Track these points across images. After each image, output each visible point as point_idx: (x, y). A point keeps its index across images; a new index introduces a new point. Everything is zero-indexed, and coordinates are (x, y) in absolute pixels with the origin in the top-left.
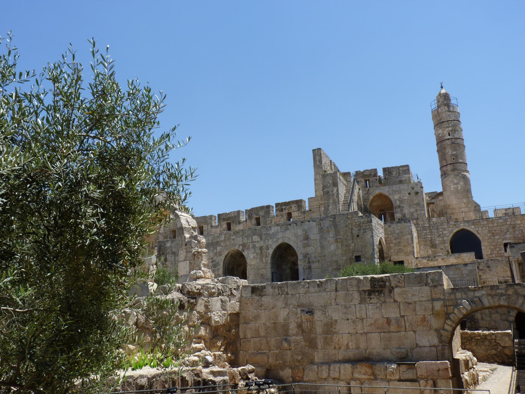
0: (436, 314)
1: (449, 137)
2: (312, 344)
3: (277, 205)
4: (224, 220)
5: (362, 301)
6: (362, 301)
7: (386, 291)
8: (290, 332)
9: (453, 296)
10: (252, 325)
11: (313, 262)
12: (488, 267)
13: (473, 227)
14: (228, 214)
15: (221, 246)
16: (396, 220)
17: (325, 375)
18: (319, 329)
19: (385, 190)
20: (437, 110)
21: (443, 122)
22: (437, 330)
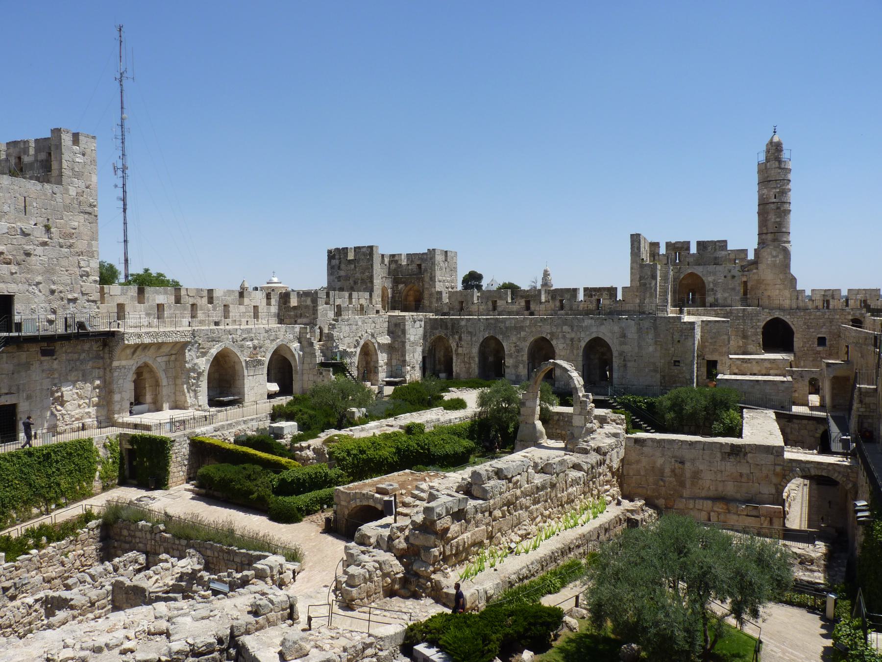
0: (776, 474)
1: (774, 200)
2: (682, 484)
3: (586, 289)
4: (522, 297)
5: (723, 459)
6: (723, 459)
7: (742, 454)
8: (665, 474)
9: (790, 465)
10: (634, 466)
11: (629, 361)
12: (802, 377)
13: (788, 317)
14: (528, 291)
15: (525, 331)
16: (708, 304)
17: (691, 506)
18: (688, 475)
19: (699, 270)
20: (766, 165)
21: (770, 181)
22: (776, 485)
